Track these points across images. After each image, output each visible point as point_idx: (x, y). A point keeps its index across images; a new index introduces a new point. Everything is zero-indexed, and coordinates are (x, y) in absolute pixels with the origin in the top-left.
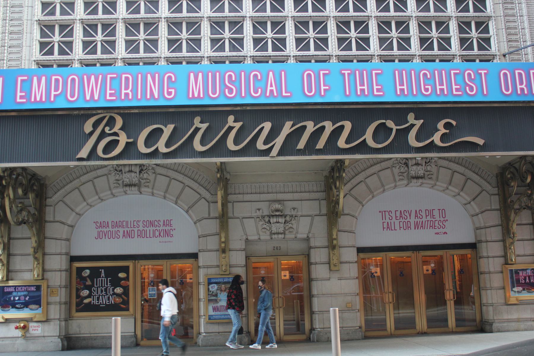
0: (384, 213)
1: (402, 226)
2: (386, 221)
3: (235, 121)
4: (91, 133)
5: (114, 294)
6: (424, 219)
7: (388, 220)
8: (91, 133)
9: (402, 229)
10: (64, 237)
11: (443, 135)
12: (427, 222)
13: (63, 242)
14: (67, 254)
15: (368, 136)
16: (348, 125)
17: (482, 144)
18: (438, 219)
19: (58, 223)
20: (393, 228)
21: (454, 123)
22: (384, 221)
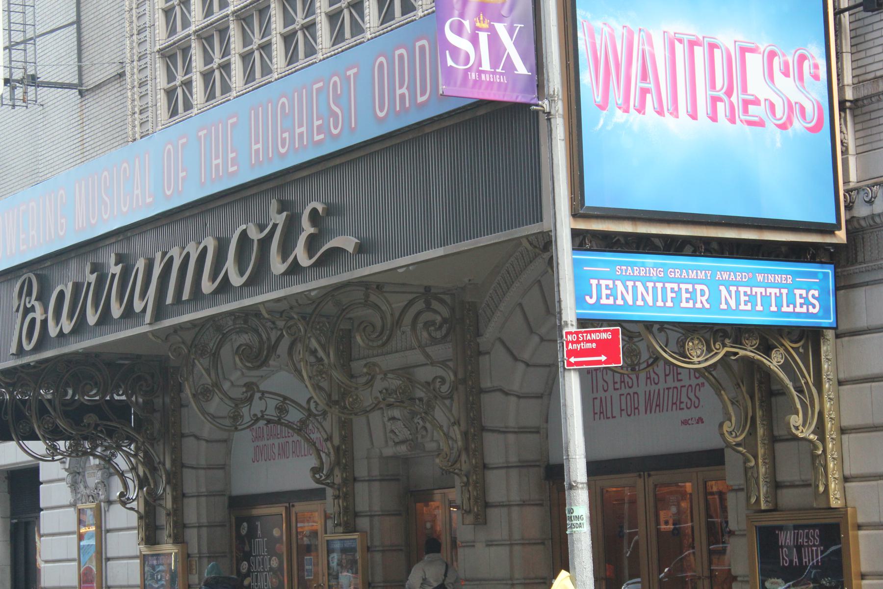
0: (594, 373)
1: (624, 407)
2: (598, 396)
3: (116, 264)
4: (17, 310)
5: (271, 569)
6: (662, 386)
7: (601, 394)
8: (17, 310)
9: (624, 413)
10: (203, 462)
11: (311, 239)
12: (666, 392)
13: (202, 472)
14: (210, 495)
15: (230, 265)
16: (210, 243)
17: (351, 249)
18: (687, 384)
19: (192, 438)
20: (609, 415)
21: (320, 207)
22: (595, 395)
